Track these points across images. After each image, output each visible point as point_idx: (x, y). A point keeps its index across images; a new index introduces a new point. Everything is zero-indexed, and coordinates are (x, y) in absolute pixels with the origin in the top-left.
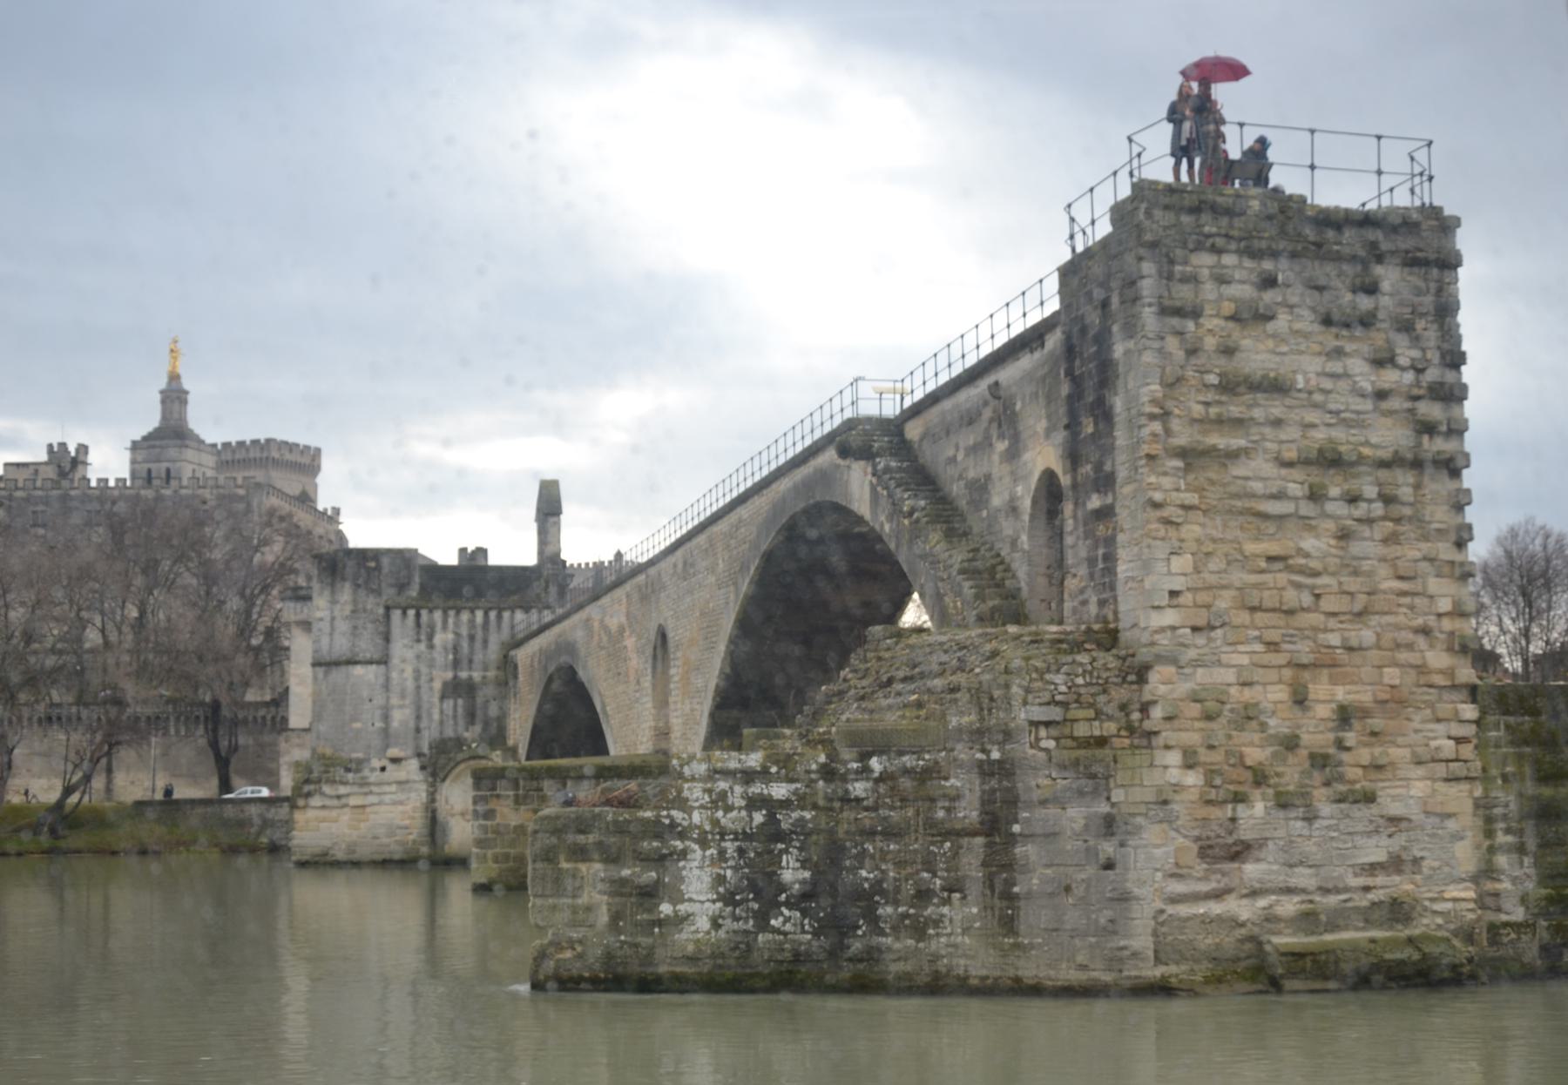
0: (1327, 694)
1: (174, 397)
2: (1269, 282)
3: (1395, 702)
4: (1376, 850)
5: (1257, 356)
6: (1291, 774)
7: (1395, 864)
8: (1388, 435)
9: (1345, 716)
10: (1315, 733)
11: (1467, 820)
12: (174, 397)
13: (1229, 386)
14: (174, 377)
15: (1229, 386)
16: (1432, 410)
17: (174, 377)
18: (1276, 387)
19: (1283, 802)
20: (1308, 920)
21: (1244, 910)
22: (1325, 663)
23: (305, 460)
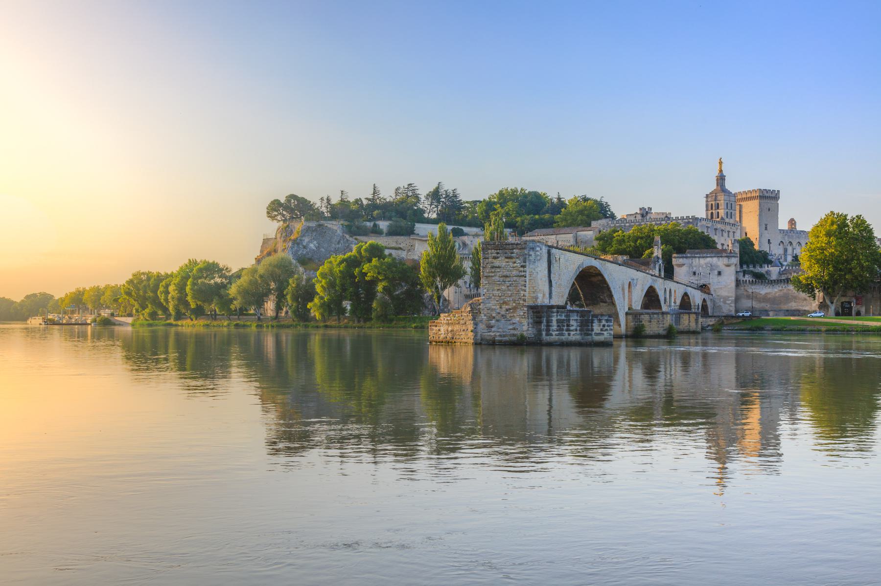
0: (505, 307)
1: (721, 179)
2: (498, 253)
3: (515, 308)
4: (511, 327)
5: (497, 263)
6: (497, 318)
7: (514, 329)
8: (515, 273)
9: (507, 310)
10: (503, 313)
11: (526, 324)
12: (721, 179)
13: (493, 267)
14: (721, 171)
15: (493, 267)
16: (522, 269)
17: (721, 171)
18: (499, 267)
19: (498, 321)
20: (500, 336)
21: (492, 334)
22: (505, 303)
23: (773, 195)
